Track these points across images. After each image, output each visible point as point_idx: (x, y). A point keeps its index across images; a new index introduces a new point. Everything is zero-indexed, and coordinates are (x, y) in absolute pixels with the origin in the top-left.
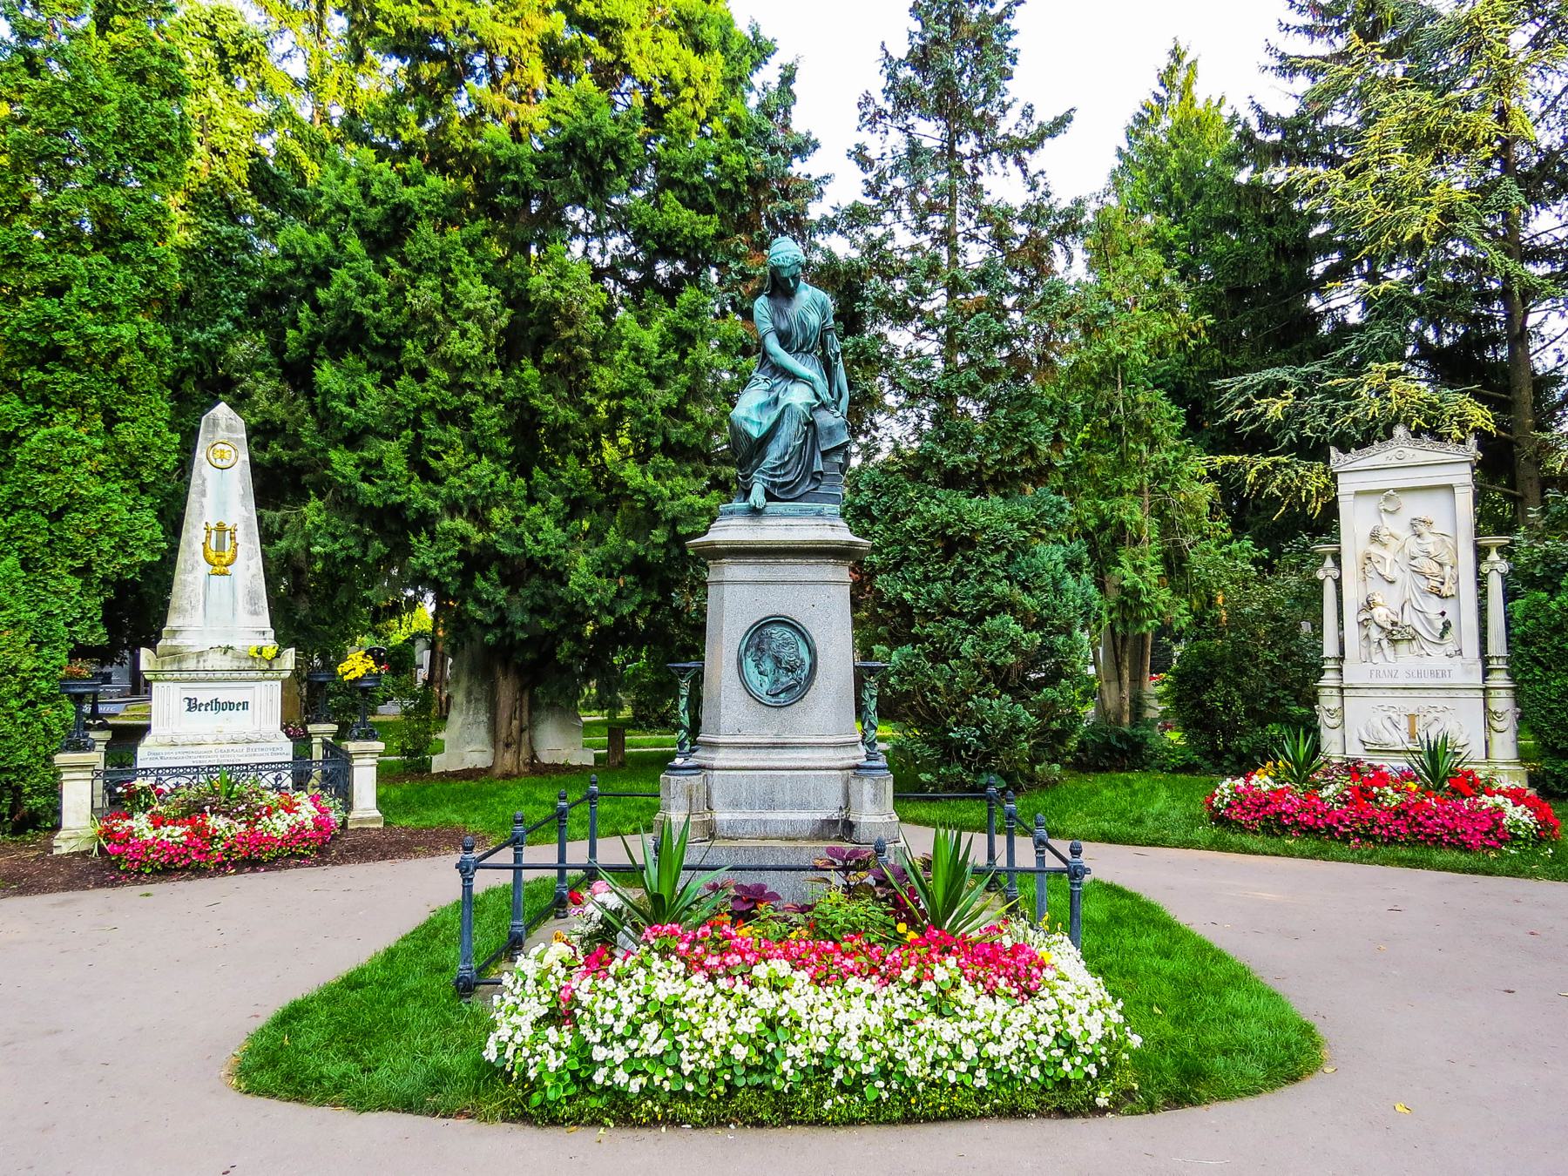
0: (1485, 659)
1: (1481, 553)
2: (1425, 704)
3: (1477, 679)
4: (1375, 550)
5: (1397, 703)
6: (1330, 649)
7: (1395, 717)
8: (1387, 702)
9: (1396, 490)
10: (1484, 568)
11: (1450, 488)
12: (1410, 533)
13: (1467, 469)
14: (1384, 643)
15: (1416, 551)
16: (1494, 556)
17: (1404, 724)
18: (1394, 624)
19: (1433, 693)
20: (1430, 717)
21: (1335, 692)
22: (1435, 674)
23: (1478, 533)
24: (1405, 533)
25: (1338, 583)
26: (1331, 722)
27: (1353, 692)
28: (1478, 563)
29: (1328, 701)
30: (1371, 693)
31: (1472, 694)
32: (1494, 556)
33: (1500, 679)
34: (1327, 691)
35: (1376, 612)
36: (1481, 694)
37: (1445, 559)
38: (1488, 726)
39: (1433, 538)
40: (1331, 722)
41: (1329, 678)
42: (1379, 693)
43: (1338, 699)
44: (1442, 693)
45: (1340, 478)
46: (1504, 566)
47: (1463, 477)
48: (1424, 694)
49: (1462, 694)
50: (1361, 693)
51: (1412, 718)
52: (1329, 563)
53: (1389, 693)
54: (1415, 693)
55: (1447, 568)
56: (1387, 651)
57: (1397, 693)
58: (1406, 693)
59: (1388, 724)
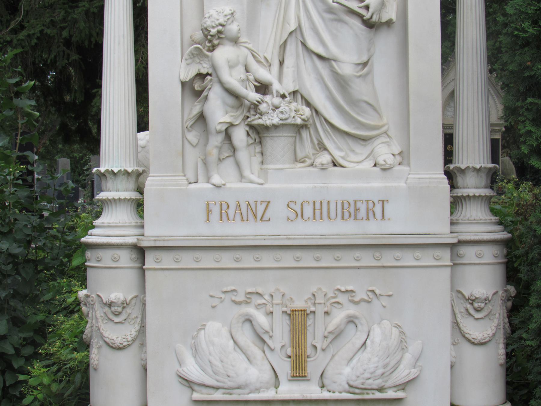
3: (436, 223)
5: (268, 285)
8: (244, 283)
14: (240, 136)
18: (263, 88)
19: (348, 259)
20: (339, 317)
21: (126, 258)
27: (167, 260)
29: (108, 283)
31: (427, 258)
33: (480, 223)
34: (106, 256)
36: (446, 256)
41: (111, 227)
42: (227, 260)
43: (132, 276)
44: (367, 258)
49: (408, 258)
50: (187, 260)
51: (298, 319)
53: (248, 260)
56: (243, 155)
59: (246, 337)
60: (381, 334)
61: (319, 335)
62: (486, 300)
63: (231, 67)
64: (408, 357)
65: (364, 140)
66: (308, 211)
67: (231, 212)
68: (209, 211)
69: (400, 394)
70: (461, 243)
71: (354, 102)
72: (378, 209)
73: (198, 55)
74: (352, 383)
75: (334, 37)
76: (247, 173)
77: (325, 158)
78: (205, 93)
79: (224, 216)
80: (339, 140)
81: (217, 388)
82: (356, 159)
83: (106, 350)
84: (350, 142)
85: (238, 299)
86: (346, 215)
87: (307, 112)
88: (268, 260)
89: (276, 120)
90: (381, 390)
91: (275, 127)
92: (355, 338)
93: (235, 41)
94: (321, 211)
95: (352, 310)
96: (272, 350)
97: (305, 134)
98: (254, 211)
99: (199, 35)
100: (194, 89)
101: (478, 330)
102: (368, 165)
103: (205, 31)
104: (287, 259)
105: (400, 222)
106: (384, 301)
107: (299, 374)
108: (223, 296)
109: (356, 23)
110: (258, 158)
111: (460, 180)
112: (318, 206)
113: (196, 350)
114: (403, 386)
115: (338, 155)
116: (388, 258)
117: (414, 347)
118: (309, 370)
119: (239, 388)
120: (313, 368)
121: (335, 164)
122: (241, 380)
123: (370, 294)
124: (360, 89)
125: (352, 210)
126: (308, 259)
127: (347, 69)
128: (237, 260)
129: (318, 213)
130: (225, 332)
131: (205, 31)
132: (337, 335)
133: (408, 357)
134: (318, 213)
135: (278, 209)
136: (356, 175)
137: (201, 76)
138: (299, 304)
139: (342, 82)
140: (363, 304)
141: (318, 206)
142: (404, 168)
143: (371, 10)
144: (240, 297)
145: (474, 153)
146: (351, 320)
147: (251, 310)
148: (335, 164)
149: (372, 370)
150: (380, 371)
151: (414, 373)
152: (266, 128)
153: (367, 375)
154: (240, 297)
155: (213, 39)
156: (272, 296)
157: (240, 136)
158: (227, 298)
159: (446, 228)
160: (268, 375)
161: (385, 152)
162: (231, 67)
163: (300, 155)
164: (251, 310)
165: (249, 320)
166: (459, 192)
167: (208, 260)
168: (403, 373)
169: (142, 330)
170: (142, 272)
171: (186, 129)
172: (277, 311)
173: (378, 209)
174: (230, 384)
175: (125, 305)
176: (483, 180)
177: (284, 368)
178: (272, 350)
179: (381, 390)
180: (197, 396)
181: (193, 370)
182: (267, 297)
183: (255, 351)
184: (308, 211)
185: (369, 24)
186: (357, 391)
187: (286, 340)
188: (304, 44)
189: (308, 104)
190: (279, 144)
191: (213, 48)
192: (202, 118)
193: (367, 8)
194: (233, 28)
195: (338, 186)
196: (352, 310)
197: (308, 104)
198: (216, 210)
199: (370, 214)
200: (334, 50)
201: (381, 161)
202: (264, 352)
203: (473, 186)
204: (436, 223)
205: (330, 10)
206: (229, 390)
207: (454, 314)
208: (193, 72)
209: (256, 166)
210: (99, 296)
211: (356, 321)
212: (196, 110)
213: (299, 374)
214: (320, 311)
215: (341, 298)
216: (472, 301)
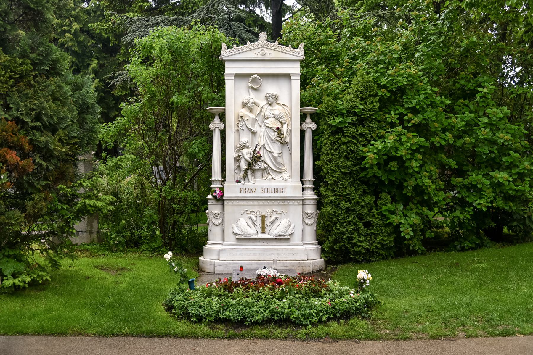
0: (302, 182)
1: (303, 117)
2: (269, 209)
3: (298, 195)
4: (244, 112)
5: (255, 209)
6: (216, 175)
7: (254, 218)
9: (258, 75)
10: (305, 126)
11: (288, 76)
12: (265, 102)
13: (298, 65)
15: (268, 113)
16: (308, 120)
17: (259, 222)
19: (276, 203)
20: (273, 217)
22: (277, 190)
23: (302, 104)
24: (263, 103)
25: (223, 133)
26: (217, 222)
27: (230, 203)
28: (301, 124)
31: (296, 203)
32: (308, 120)
35: (245, 151)
36: (301, 202)
37: (284, 120)
38: (303, 220)
39: (277, 107)
40: (217, 222)
42: (245, 203)
44: (281, 203)
45: (227, 65)
46: (314, 126)
47: (295, 70)
50: (235, 203)
51: (263, 219)
52: (217, 119)
53: (251, 203)
55: (285, 126)
56: (249, 176)
59: (250, 222)
60: (284, 222)
61: (268, 222)
62: (311, 214)
63: (247, 154)
64: (291, 228)
65: (280, 173)
66: (266, 191)
69: (289, 237)
70: (304, 199)
71: (278, 163)
72: (284, 190)
73: (238, 151)
75: (273, 146)
76: (250, 181)
77: (270, 177)
80: (274, 173)
82: (278, 177)
83: (213, 225)
87: (266, 166)
88: (256, 203)
89: (258, 168)
91: (258, 169)
92: (277, 223)
93: (248, 147)
94: (269, 190)
95: (277, 216)
97: (265, 171)
98: (252, 191)
99: (238, 145)
100: (237, 159)
101: (309, 222)
102: (281, 179)
103: (241, 145)
104: (261, 203)
105: (289, 194)
106: (285, 214)
107: (263, 232)
109: (279, 143)
110: (253, 177)
111: (305, 183)
113: (237, 225)
114: (290, 235)
115: (273, 176)
116: (286, 203)
117: (292, 225)
120: (267, 230)
121: (273, 178)
122: (249, 233)
124: (280, 160)
126: (266, 203)
127: (276, 155)
130: (245, 221)
131: (241, 145)
132: (273, 222)
133: (291, 228)
135: (259, 190)
136: (277, 182)
137: (239, 156)
138: (263, 214)
139: (275, 158)
142: (290, 180)
145: (309, 176)
146: (277, 218)
147: (251, 215)
148: (273, 178)
151: (292, 232)
152: (256, 170)
155: (243, 147)
157: (249, 172)
159: (301, 195)
160: (255, 232)
161: (285, 175)
162: (247, 154)
163: (264, 176)
164: (251, 215)
165: (251, 218)
166: (304, 186)
167: (240, 203)
168: (290, 232)
169: (223, 221)
170: (224, 206)
171: (235, 169)
172: (258, 216)
173: (284, 190)
175: (219, 214)
176: (311, 183)
177: (260, 230)
179: (284, 236)
180: (237, 237)
181: (237, 231)
183: (252, 226)
184: (266, 191)
185: (282, 143)
187: (260, 223)
189: (266, 163)
190: (259, 174)
191: (242, 149)
192: (239, 166)
194: (248, 144)
195: (273, 184)
196: (277, 216)
197: (266, 163)
198: (243, 190)
199: (281, 192)
200: (273, 150)
203: (309, 185)
204: (298, 195)
205: (272, 140)
206: (246, 235)
207: (303, 217)
208: (237, 155)
209: (253, 179)
212: (237, 165)
213: (263, 232)
214: (269, 216)
216: (308, 214)
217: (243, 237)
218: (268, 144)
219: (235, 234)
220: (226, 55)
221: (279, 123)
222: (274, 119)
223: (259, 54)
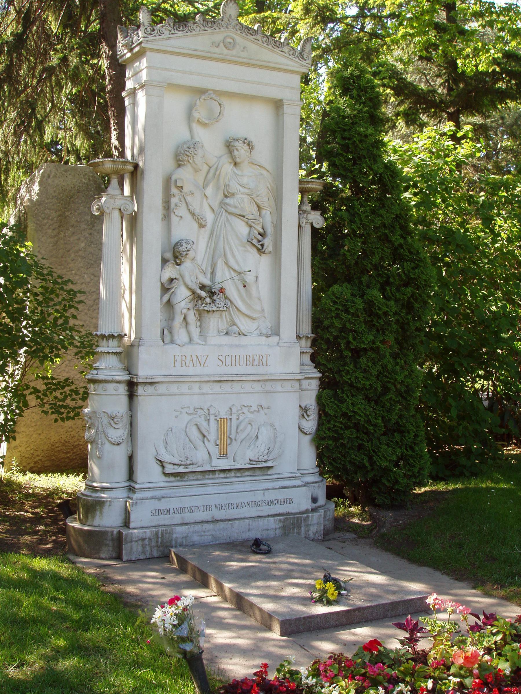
19: (247, 387)
21: (123, 389)
22: (250, 361)
27: (150, 389)
30: (174, 389)
31: (288, 386)
42: (184, 388)
43: (124, 400)
44: (258, 387)
48: (237, 387)
49: (278, 386)
50: (161, 388)
54: (227, 387)
57: (206, 388)
58: (217, 388)
59: (194, 434)
65: (253, 319)
67: (188, 360)
68: (175, 361)
72: (264, 360)
74: (252, 459)
78: (173, 290)
79: (183, 363)
81: (181, 465)
84: (247, 320)
85: (190, 412)
86: (248, 362)
89: (214, 308)
90: (266, 461)
95: (251, 416)
96: (209, 441)
106: (266, 411)
108: (182, 410)
112: (234, 358)
114: (274, 460)
116: (268, 386)
118: (228, 452)
119: (193, 464)
120: (231, 451)
123: (259, 408)
125: (251, 360)
128: (190, 389)
129: (234, 362)
134: (234, 362)
137: (171, 280)
140: (255, 413)
141: (234, 358)
143: (265, 247)
144: (191, 411)
149: (262, 451)
150: (266, 451)
153: (261, 454)
154: (191, 411)
156: (209, 410)
158: (184, 411)
174: (188, 462)
177: (215, 451)
178: (209, 441)
179: (266, 461)
182: (206, 411)
186: (254, 463)
188: (227, 264)
193: (262, 245)
198: (179, 359)
201: (264, 332)
202: (204, 443)
206: (186, 466)
209: (198, 333)
210: (104, 412)
211: (253, 423)
213: (223, 455)
215: (245, 410)
217: (181, 469)
218: (233, 256)
219: (161, 463)
220: (150, 38)
221: (256, 207)
222: (246, 199)
223: (222, 45)
